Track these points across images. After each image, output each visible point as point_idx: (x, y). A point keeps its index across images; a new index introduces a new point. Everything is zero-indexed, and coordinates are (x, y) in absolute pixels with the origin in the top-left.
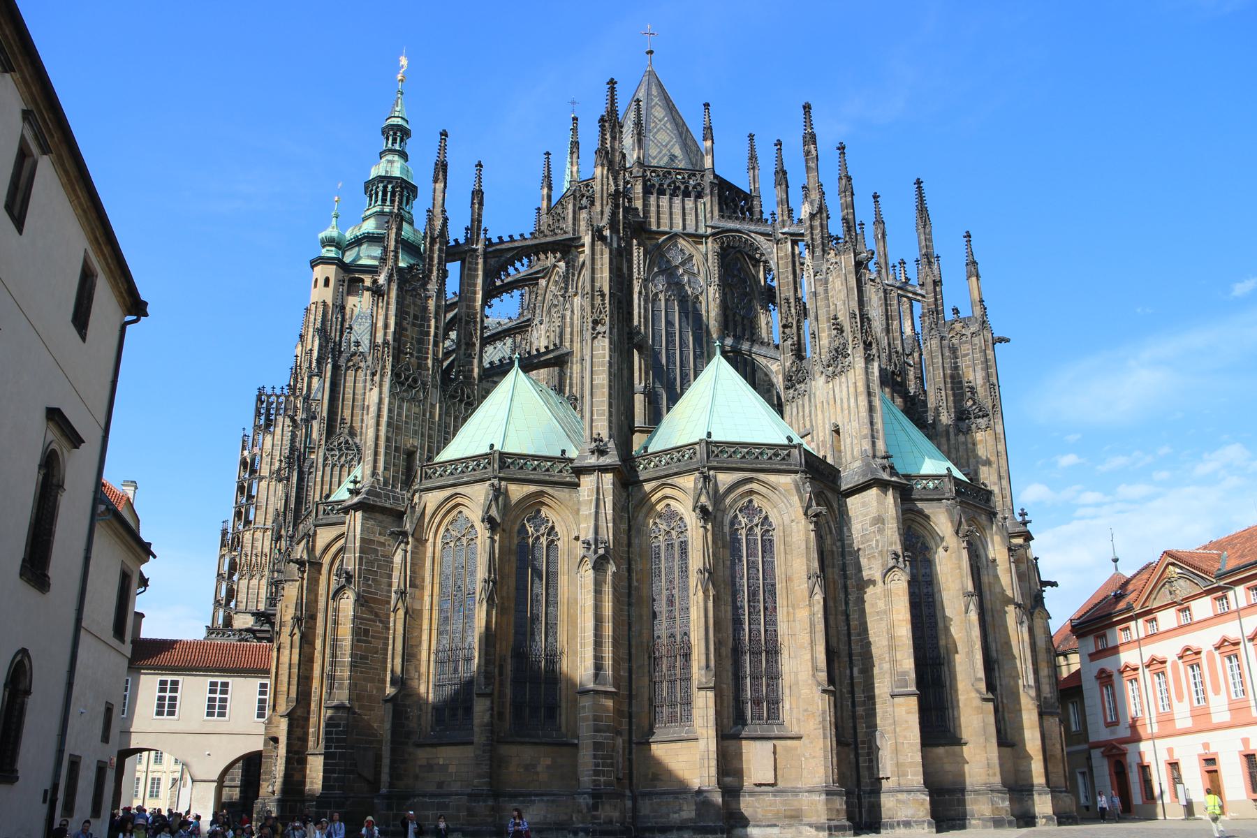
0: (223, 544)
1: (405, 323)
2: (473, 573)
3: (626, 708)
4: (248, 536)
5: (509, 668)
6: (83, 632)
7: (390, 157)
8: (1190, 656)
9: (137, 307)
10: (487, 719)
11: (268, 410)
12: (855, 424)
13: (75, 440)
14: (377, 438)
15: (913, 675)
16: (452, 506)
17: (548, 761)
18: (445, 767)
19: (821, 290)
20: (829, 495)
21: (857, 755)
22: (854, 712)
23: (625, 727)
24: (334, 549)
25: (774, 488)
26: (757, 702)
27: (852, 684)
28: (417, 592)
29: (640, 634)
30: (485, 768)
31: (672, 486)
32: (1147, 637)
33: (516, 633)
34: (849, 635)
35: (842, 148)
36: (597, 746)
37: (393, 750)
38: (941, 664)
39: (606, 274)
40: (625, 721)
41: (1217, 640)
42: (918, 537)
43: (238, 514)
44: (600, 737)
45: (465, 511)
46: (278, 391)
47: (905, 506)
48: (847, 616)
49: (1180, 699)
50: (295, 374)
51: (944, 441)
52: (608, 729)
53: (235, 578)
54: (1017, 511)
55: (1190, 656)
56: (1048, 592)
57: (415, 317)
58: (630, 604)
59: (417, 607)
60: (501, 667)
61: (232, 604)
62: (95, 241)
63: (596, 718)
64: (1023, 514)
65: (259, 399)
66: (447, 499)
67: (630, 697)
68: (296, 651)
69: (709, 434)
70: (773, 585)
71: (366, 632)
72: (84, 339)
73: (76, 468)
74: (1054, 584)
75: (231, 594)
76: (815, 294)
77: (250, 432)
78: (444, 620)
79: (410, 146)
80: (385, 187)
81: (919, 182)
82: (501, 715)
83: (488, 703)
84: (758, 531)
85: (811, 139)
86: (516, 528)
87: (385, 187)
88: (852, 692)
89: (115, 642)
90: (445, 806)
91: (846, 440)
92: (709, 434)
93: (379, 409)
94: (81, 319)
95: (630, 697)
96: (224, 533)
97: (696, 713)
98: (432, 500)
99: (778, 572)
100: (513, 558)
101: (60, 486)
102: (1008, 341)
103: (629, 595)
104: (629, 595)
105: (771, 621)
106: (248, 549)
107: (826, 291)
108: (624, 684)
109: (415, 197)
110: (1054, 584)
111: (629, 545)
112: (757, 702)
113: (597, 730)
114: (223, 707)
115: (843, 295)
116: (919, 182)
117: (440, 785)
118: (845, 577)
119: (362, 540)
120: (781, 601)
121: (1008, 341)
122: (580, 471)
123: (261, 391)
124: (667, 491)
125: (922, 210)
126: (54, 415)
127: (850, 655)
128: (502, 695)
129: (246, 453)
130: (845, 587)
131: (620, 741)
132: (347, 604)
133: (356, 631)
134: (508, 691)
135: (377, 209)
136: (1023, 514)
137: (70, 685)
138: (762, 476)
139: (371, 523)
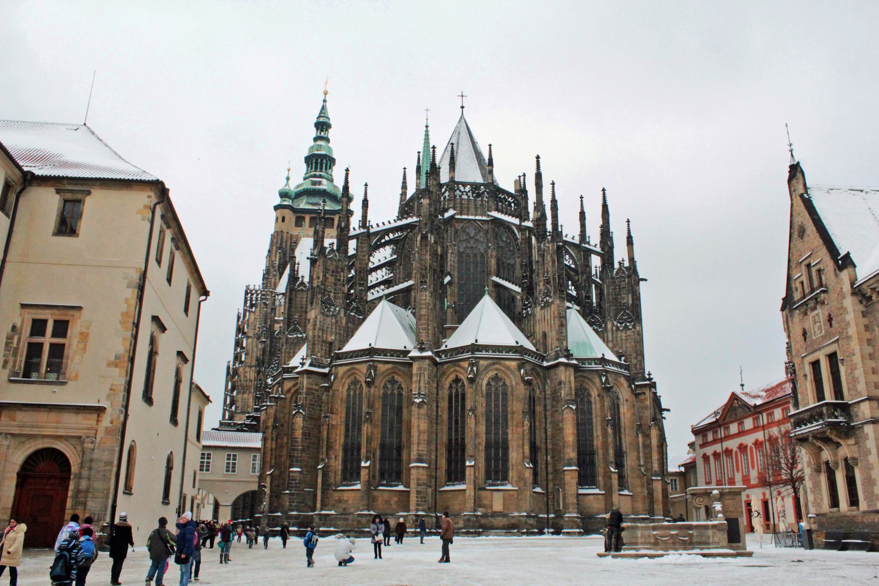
0: (228, 373)
1: (327, 275)
2: (360, 408)
3: (434, 474)
4: (241, 369)
5: (378, 453)
6: (188, 443)
7: (319, 143)
8: (743, 448)
9: (206, 293)
10: (367, 478)
11: (251, 298)
12: (554, 333)
13: (186, 360)
14: (314, 336)
15: (575, 461)
16: (351, 373)
17: (396, 499)
18: (347, 501)
19: (541, 259)
20: (538, 369)
21: (548, 499)
22: (547, 477)
23: (433, 483)
24: (292, 391)
25: (508, 368)
26: (496, 472)
27: (547, 464)
28: (334, 416)
29: (442, 439)
30: (366, 502)
31: (459, 366)
32: (725, 437)
33: (382, 437)
34: (546, 439)
35: (553, 184)
36: (418, 492)
37: (322, 493)
38: (594, 454)
39: (428, 257)
40: (433, 480)
41: (753, 441)
42: (585, 389)
43: (237, 357)
44: (419, 488)
45: (358, 377)
46: (257, 288)
47: (579, 374)
48: (546, 430)
49: (738, 471)
50: (266, 276)
51: (610, 334)
52: (424, 484)
53: (235, 393)
54: (647, 372)
55: (743, 448)
56: (665, 414)
57: (333, 271)
58: (437, 424)
59: (334, 423)
60: (374, 454)
61: (233, 408)
62: (192, 274)
63: (418, 479)
64: (649, 374)
65: (247, 293)
66: (348, 370)
67: (436, 468)
68: (274, 442)
69: (476, 341)
70: (507, 416)
71: (309, 434)
72: (187, 315)
73: (186, 369)
74: (668, 410)
75: (233, 402)
76: (538, 262)
77: (242, 311)
78: (347, 430)
79: (331, 134)
80: (317, 160)
81: (604, 190)
82: (374, 476)
83: (367, 471)
84: (500, 389)
85: (539, 176)
86: (382, 385)
87: (317, 160)
88: (547, 468)
89: (197, 443)
90: (347, 519)
91: (549, 341)
92: (476, 341)
93: (315, 321)
94: (186, 310)
95: (436, 468)
96: (228, 368)
97: (467, 477)
98: (341, 370)
99: (509, 409)
100: (381, 401)
101: (181, 381)
102: (646, 280)
103: (437, 419)
104: (437, 419)
105: (507, 434)
106: (242, 377)
107: (543, 260)
108: (433, 462)
109: (334, 164)
110: (668, 410)
111: (437, 394)
112: (496, 472)
113: (418, 485)
114: (234, 467)
115: (550, 264)
116: (604, 190)
117: (345, 509)
118: (546, 410)
119: (308, 388)
120: (510, 424)
121: (646, 280)
122: (412, 358)
123: (248, 287)
124: (457, 368)
125: (605, 207)
126: (180, 354)
127: (546, 450)
128: (374, 467)
129: (240, 323)
130: (545, 416)
131: (430, 490)
132: (299, 421)
133: (304, 434)
134: (378, 467)
135: (313, 173)
136: (649, 374)
137: (184, 464)
138: (502, 362)
139: (311, 380)
